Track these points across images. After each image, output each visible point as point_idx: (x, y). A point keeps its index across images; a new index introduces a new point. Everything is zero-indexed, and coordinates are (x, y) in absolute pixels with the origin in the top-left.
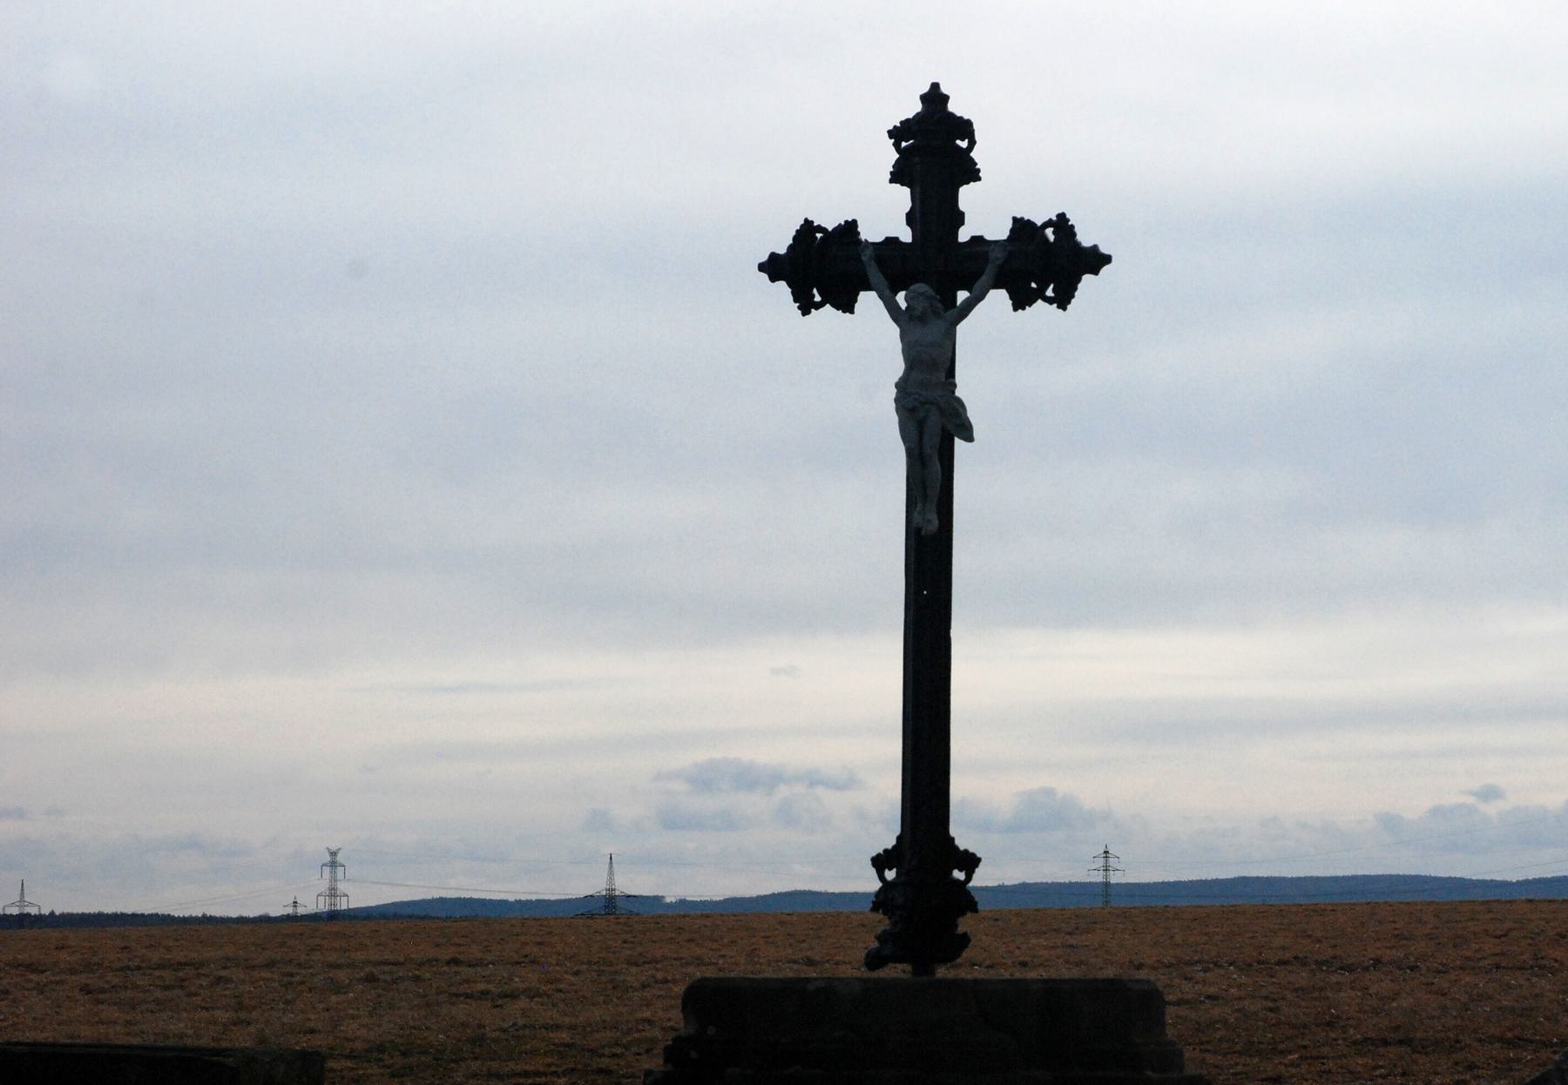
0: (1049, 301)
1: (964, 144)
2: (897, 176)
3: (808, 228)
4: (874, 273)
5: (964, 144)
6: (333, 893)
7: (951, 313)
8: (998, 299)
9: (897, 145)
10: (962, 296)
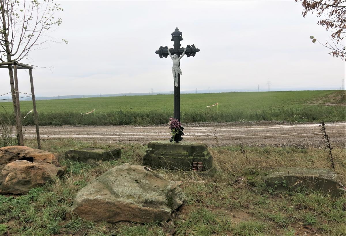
0: (192, 56)
1: (181, 35)
2: (172, 40)
3: (161, 47)
4: (169, 53)
5: (181, 35)
6: (152, 91)
7: (179, 58)
8: (186, 55)
9: (172, 36)
10: (181, 55)
